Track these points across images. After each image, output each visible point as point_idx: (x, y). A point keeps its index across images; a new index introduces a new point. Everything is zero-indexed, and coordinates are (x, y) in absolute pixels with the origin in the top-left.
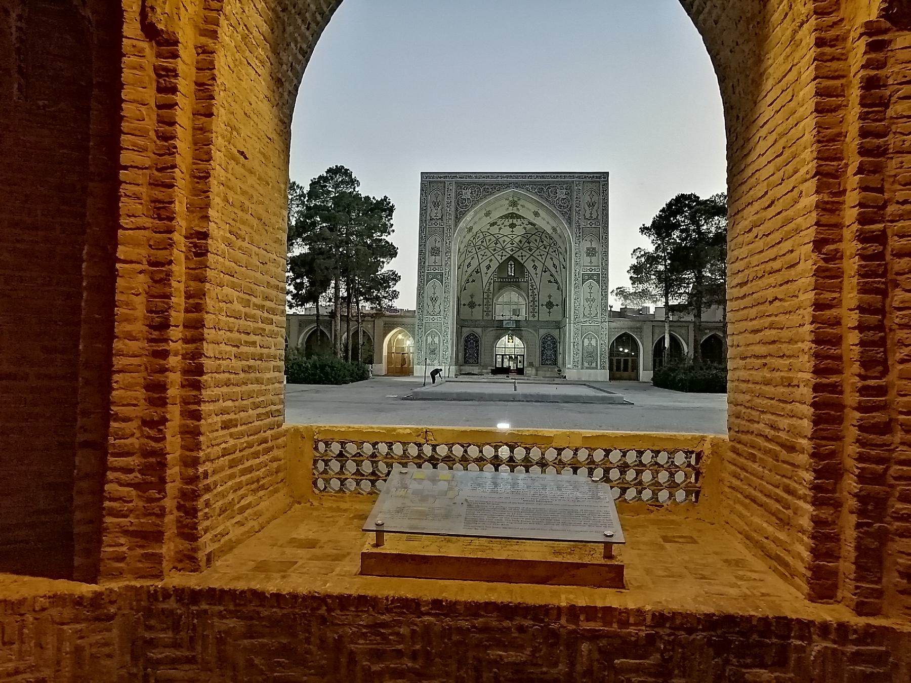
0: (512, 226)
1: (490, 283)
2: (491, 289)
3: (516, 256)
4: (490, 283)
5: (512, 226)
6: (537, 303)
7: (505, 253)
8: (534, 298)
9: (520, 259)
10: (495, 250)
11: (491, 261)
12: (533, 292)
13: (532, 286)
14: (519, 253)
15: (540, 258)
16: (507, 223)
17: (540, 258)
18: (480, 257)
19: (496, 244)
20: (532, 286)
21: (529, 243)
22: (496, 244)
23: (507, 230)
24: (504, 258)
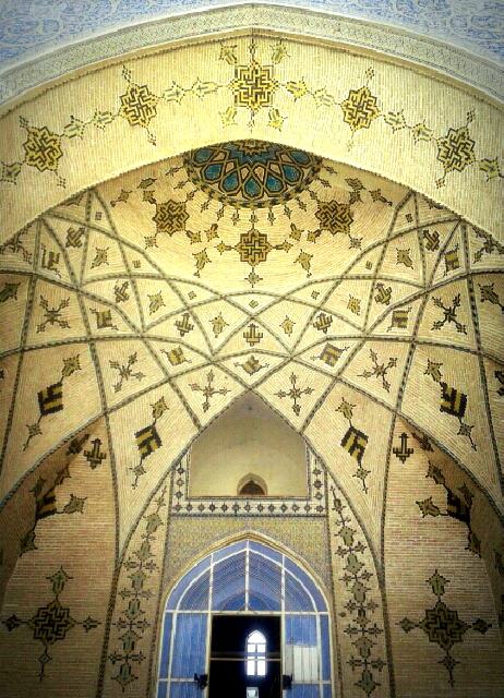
0: (254, 247)
1: (154, 522)
2: (157, 547)
3: (268, 391)
4: (154, 522)
5: (254, 247)
6: (375, 617)
7: (220, 380)
8: (360, 592)
9: (284, 407)
10: (177, 357)
11: (159, 409)
12: (353, 564)
13: (347, 535)
14: (281, 381)
15: (373, 385)
16: (231, 234)
17: (373, 385)
18: (112, 376)
19: (184, 328)
20: (347, 535)
21: (324, 324)
22: (184, 328)
23: (228, 272)
24: (219, 404)
